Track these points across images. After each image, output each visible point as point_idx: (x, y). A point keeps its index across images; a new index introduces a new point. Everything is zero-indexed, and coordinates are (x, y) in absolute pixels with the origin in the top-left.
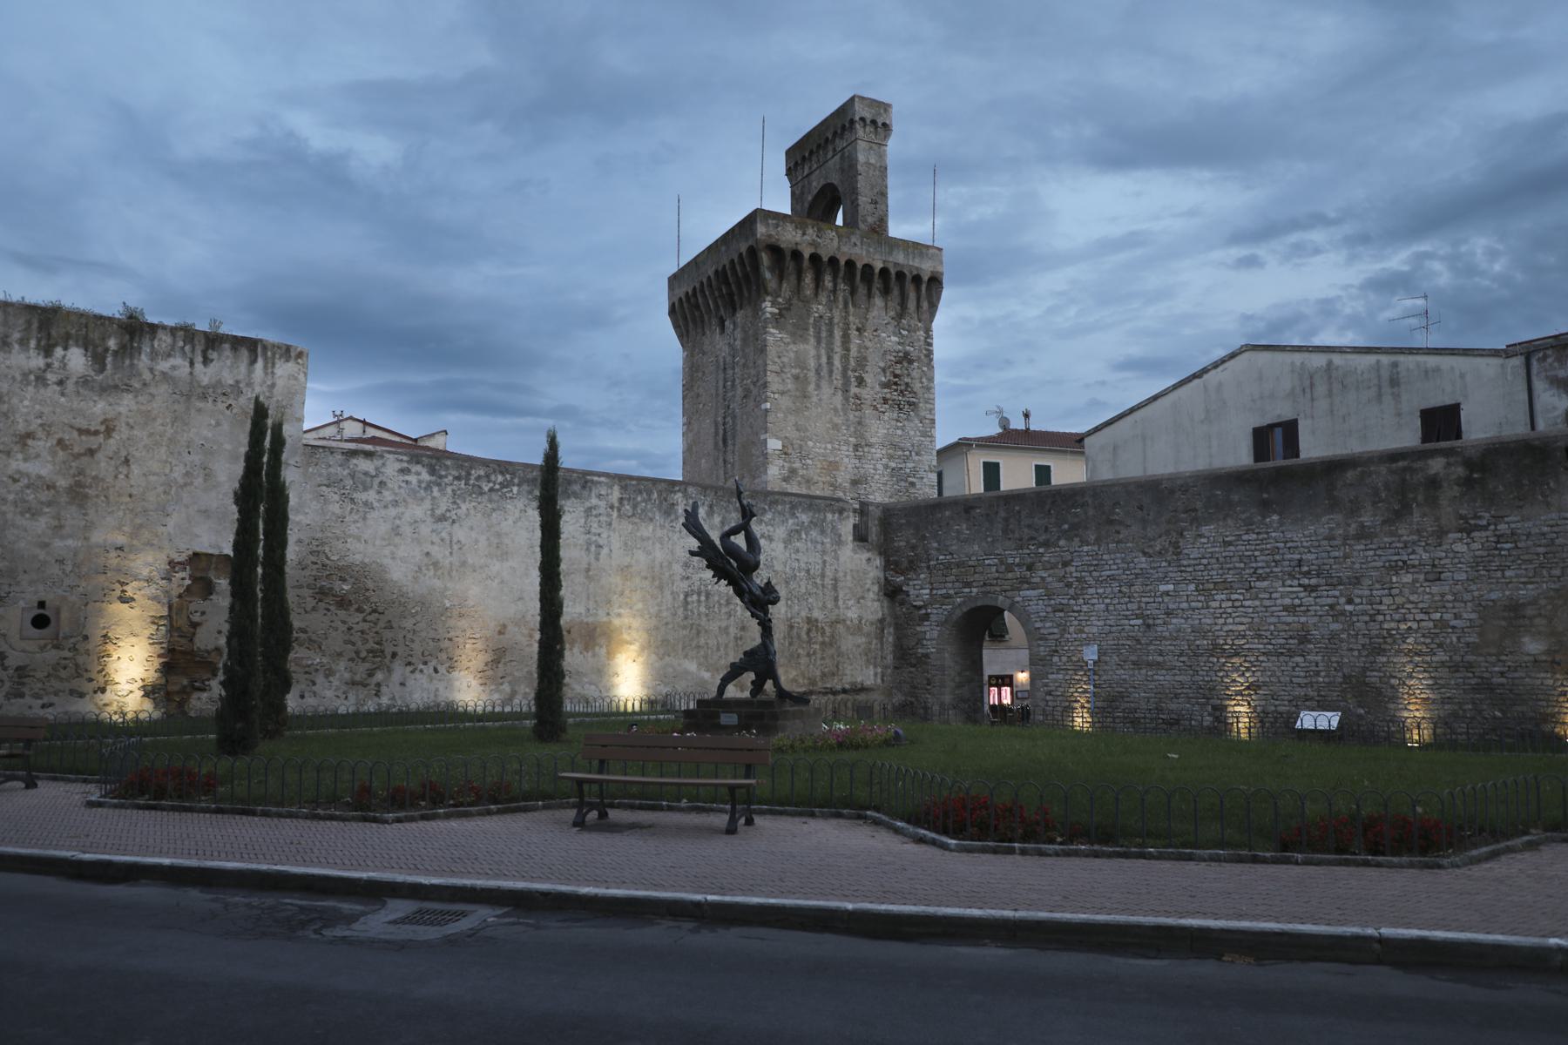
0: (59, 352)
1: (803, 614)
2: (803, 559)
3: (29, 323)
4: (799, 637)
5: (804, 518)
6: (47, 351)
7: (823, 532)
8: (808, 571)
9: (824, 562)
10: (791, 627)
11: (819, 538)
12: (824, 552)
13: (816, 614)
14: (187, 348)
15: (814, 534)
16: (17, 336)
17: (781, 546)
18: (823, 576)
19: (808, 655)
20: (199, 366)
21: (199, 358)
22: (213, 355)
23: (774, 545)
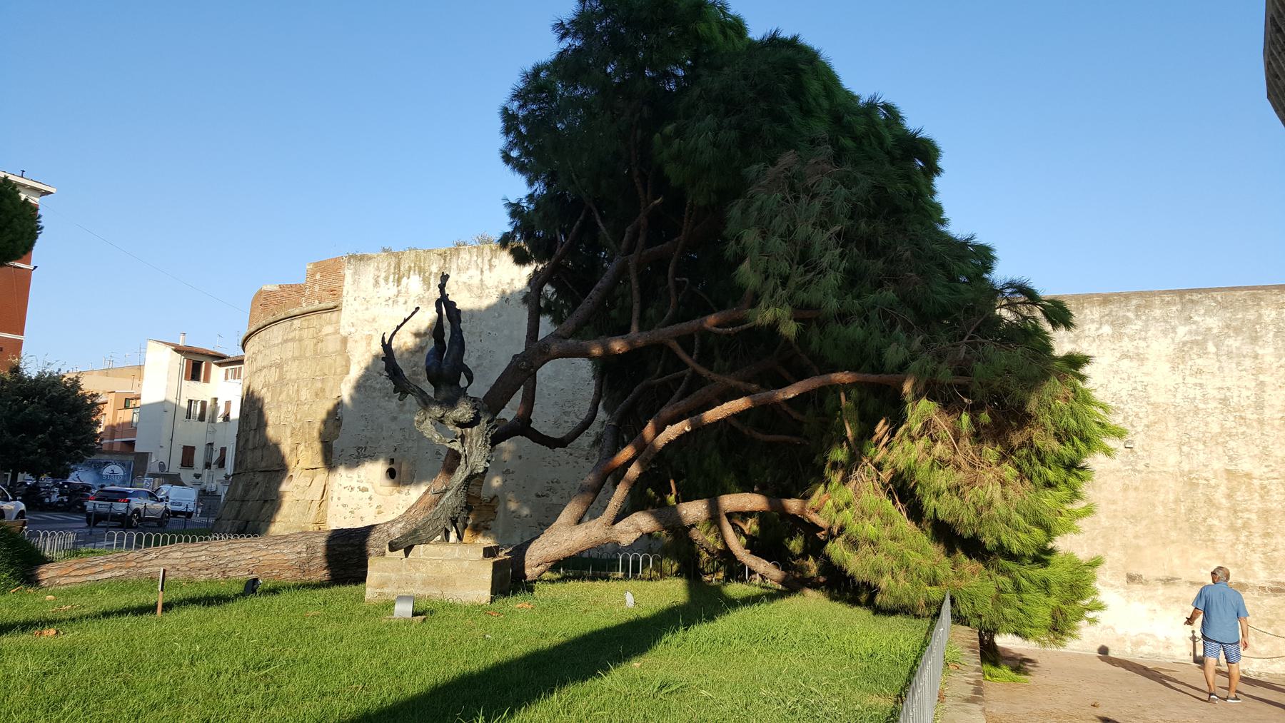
0: (404, 281)
1: (1218, 465)
2: (1212, 385)
3: (389, 265)
4: (1210, 501)
5: (1214, 323)
6: (399, 281)
7: (1254, 339)
8: (1224, 401)
9: (1262, 384)
10: (1193, 485)
11: (1247, 349)
12: (1259, 370)
13: (1245, 465)
14: (480, 261)
15: (1233, 343)
16: (383, 275)
17: (1165, 367)
18: (1259, 406)
19: (1233, 528)
20: (486, 273)
21: (486, 267)
22: (495, 261)
23: (1148, 367)
